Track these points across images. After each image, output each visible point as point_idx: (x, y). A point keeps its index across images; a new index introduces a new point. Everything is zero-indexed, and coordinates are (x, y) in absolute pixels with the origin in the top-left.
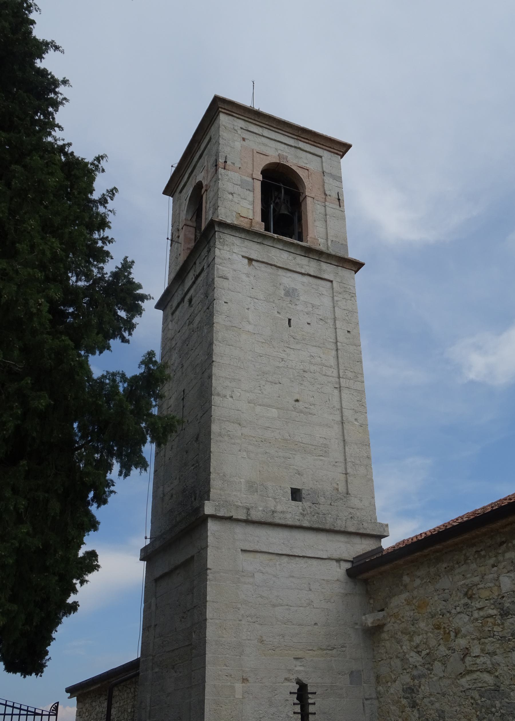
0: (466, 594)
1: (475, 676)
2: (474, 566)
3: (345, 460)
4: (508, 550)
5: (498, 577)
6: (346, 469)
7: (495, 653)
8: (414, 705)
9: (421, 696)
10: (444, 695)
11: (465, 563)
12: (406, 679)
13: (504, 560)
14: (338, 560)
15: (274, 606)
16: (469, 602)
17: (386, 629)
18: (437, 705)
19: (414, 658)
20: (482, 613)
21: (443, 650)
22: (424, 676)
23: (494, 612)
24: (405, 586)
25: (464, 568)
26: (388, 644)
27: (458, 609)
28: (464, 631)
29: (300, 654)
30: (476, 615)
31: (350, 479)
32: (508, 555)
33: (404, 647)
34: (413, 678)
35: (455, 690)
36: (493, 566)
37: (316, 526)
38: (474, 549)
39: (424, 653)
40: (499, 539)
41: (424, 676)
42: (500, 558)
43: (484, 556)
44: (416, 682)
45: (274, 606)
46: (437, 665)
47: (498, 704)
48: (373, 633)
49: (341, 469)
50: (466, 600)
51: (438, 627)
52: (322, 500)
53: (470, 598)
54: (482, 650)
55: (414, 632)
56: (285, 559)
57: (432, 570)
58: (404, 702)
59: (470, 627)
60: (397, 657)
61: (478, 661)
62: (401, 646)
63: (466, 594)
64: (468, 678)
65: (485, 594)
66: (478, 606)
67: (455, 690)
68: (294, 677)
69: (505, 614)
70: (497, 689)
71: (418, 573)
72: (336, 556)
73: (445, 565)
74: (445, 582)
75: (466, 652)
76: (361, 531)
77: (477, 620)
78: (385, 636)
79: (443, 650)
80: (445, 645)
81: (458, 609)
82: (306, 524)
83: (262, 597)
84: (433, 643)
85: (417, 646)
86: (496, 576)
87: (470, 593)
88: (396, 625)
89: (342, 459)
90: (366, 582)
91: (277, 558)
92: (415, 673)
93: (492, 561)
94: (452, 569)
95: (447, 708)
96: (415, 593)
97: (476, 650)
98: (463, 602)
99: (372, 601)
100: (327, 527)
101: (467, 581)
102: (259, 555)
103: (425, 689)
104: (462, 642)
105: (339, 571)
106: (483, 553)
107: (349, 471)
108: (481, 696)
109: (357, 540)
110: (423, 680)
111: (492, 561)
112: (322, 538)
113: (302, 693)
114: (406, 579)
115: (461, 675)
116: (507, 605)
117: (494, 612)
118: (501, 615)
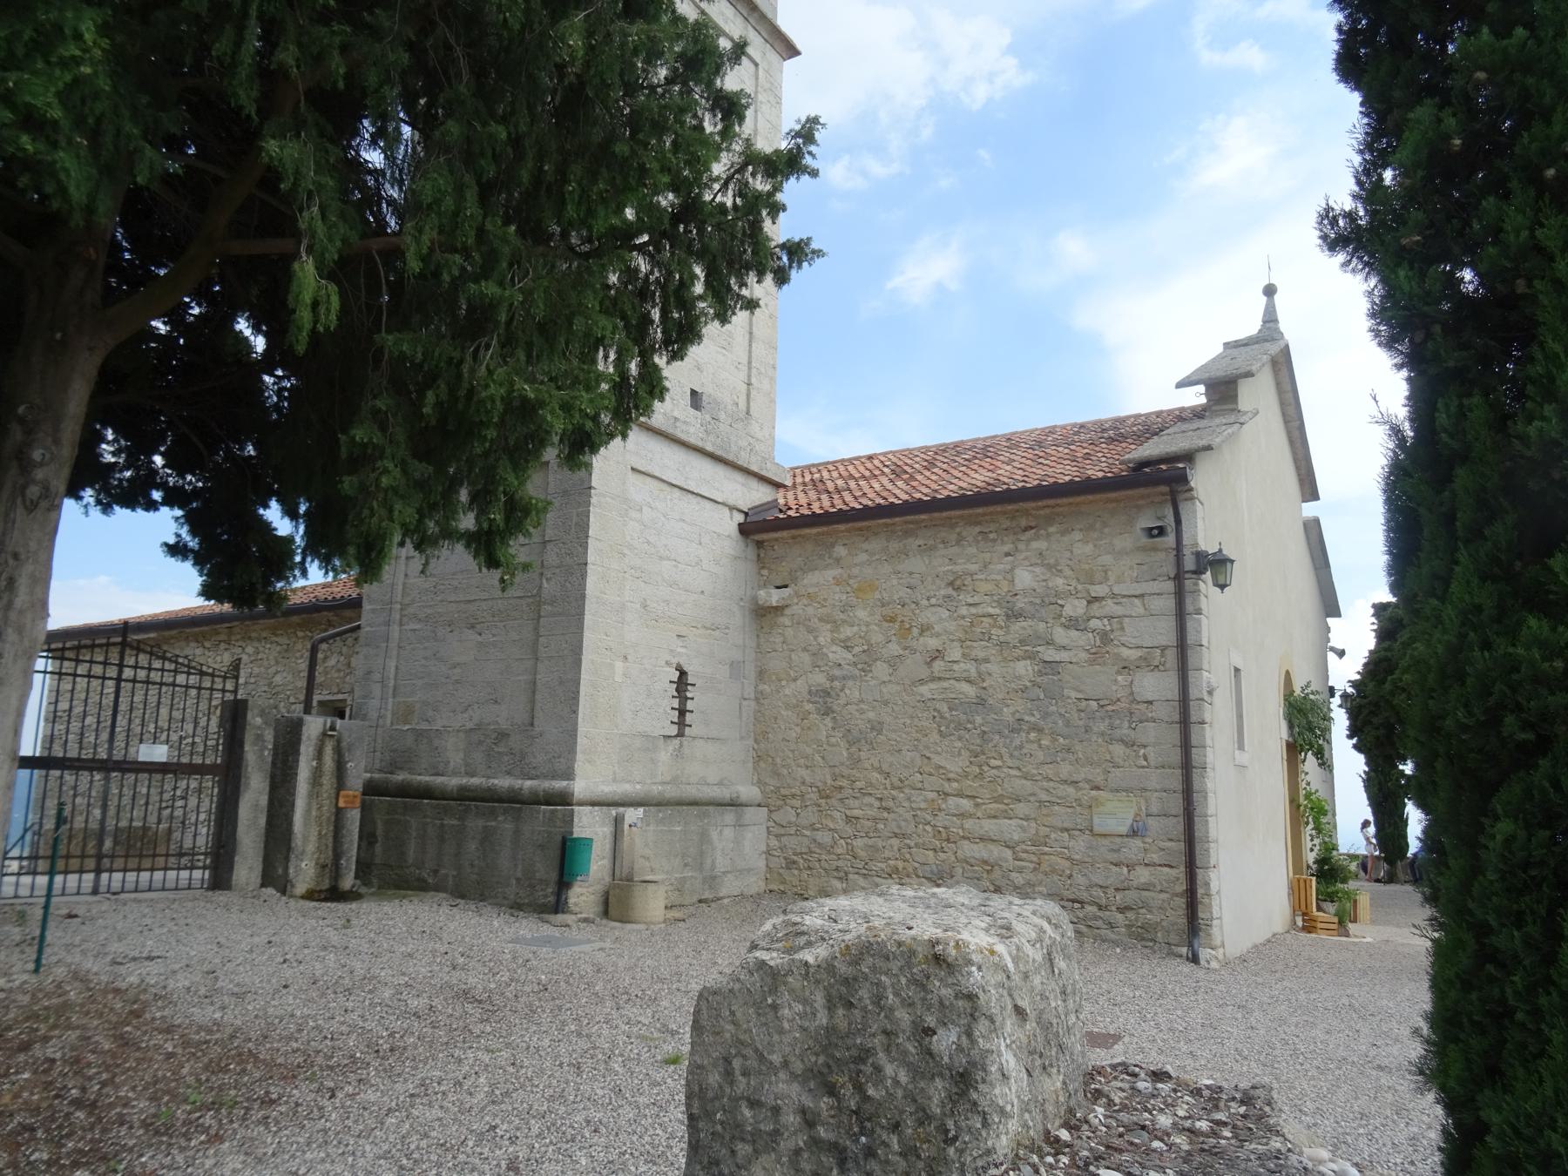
0: (951, 584)
1: (945, 684)
2: (973, 550)
3: (750, 363)
4: (1037, 537)
5: (1012, 569)
6: (749, 376)
7: (987, 661)
8: (827, 711)
9: (842, 702)
10: (886, 703)
11: (958, 542)
12: (819, 679)
13: (1027, 550)
14: (732, 508)
15: (661, 558)
16: (954, 594)
17: (788, 611)
18: (871, 715)
19: (837, 654)
20: (973, 610)
21: (895, 648)
22: (853, 678)
23: (997, 611)
24: (838, 560)
25: (956, 549)
26: (790, 632)
27: (933, 601)
28: (937, 628)
29: (684, 631)
30: (964, 611)
31: (753, 393)
32: (1035, 545)
33: (821, 639)
34: (832, 679)
35: (906, 698)
36: (1008, 554)
37: (719, 453)
38: (978, 529)
39: (857, 650)
40: (1024, 523)
41: (853, 678)
42: (1021, 546)
43: (994, 541)
44: (836, 684)
45: (661, 558)
46: (881, 670)
47: (978, 720)
48: (763, 615)
49: (743, 375)
50: (950, 591)
51: (892, 620)
52: (722, 416)
53: (957, 589)
54: (964, 655)
55: (844, 621)
56: (677, 493)
57: (894, 546)
58: (809, 707)
59: (951, 626)
60: (805, 650)
61: (956, 667)
62: (816, 638)
63: (951, 584)
64: (933, 686)
65: (985, 587)
66: (970, 601)
67: (906, 698)
68: (675, 661)
69: (1013, 615)
70: (981, 702)
71: (865, 546)
72: (731, 502)
73: (918, 542)
74: (917, 564)
75: (938, 655)
76: (763, 473)
77: (963, 617)
78: (785, 621)
79: (895, 648)
80: (899, 643)
81: (933, 601)
82: (709, 448)
83: (648, 543)
84: (877, 638)
85: (848, 639)
86: (1008, 567)
87: (958, 582)
88: (810, 611)
89: (745, 361)
90: (759, 544)
91: (668, 488)
92: (837, 672)
93: (1007, 548)
94: (933, 548)
95: (888, 719)
96: (856, 571)
97: (955, 653)
98: (942, 592)
99: (765, 572)
100: (730, 457)
101: (958, 568)
102: (649, 480)
103: (853, 692)
104: (933, 643)
105: (729, 524)
106: (992, 536)
107: (753, 380)
108: (951, 709)
109: (754, 483)
110: (850, 683)
111: (1007, 548)
112: (720, 471)
113: (682, 682)
114: (840, 551)
115: (922, 682)
116: (1020, 605)
117: (997, 611)
118: (1007, 616)
